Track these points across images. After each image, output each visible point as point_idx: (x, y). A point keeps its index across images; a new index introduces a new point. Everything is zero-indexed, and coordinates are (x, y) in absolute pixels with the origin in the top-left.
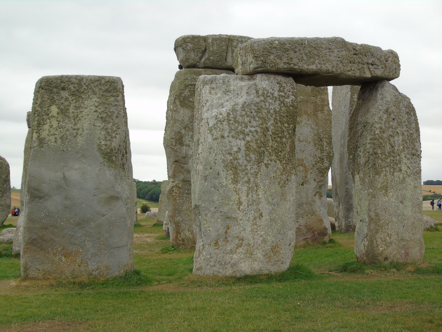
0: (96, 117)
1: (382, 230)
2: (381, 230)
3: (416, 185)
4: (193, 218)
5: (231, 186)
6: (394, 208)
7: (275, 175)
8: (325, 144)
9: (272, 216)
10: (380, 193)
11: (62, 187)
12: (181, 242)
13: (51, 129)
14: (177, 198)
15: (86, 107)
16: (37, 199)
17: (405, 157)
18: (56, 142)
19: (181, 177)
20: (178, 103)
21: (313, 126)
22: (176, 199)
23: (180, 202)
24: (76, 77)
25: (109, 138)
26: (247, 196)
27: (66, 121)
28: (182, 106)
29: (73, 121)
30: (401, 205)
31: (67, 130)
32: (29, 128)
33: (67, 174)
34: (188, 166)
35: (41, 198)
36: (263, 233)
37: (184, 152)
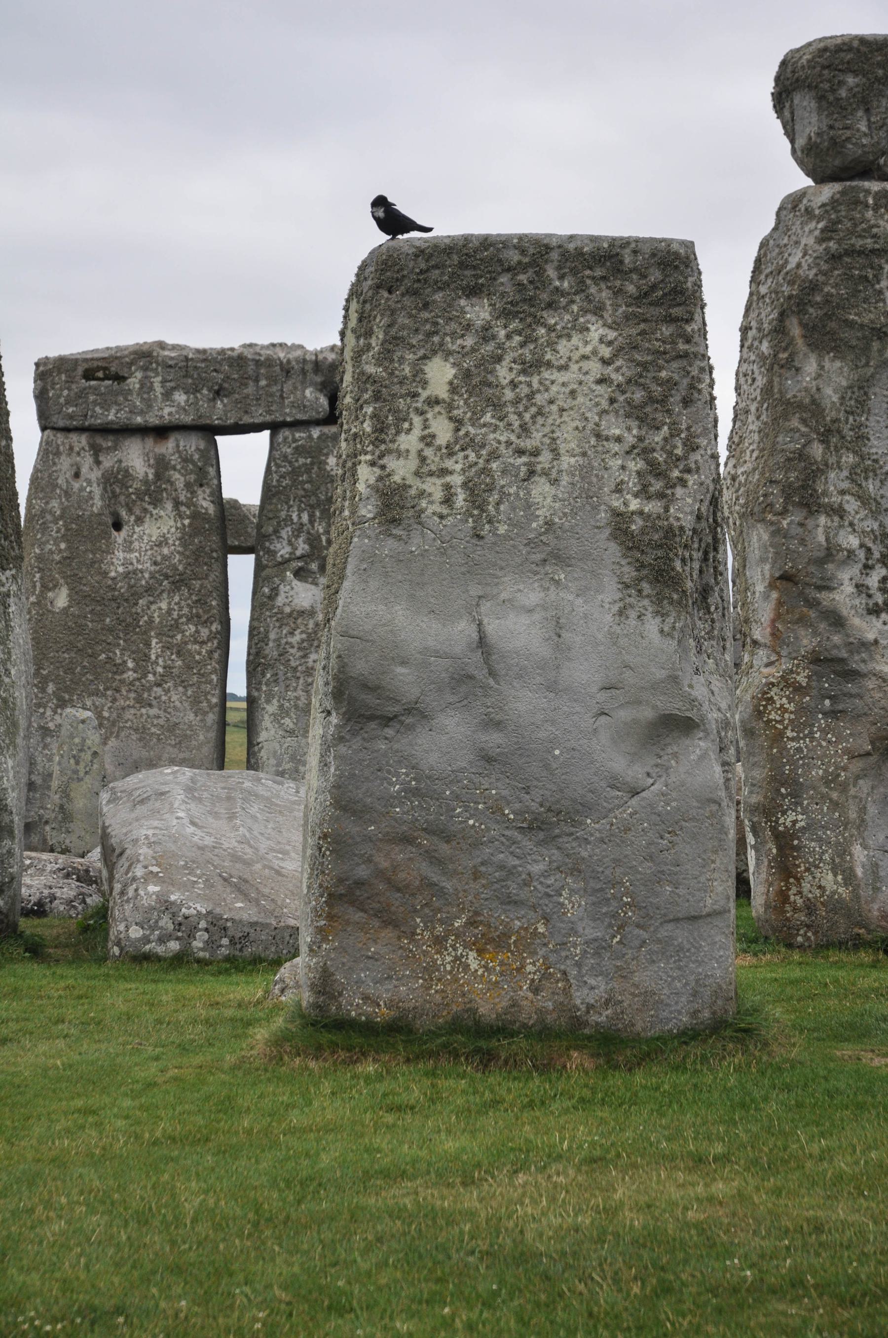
0: (605, 404)
4: (853, 815)
11: (471, 677)
13: (428, 452)
14: (789, 734)
15: (562, 362)
16: (373, 725)
18: (448, 500)
19: (805, 642)
20: (796, 331)
22: (781, 734)
23: (799, 750)
24: (522, 243)
25: (657, 485)
27: (488, 418)
28: (814, 346)
29: (513, 418)
31: (494, 455)
32: (43, 429)
33: (492, 627)
35: (387, 720)
37: (821, 538)
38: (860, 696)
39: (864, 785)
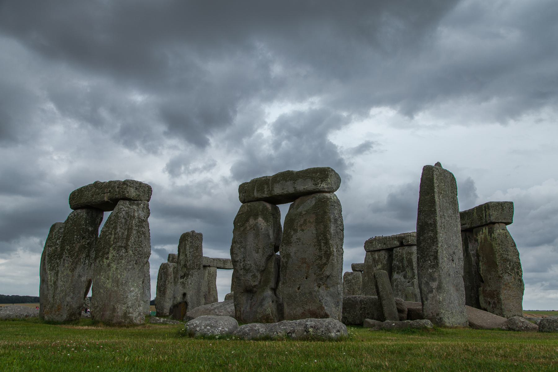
5: (49, 272)
8: (322, 244)
30: (108, 281)
39: (244, 298)
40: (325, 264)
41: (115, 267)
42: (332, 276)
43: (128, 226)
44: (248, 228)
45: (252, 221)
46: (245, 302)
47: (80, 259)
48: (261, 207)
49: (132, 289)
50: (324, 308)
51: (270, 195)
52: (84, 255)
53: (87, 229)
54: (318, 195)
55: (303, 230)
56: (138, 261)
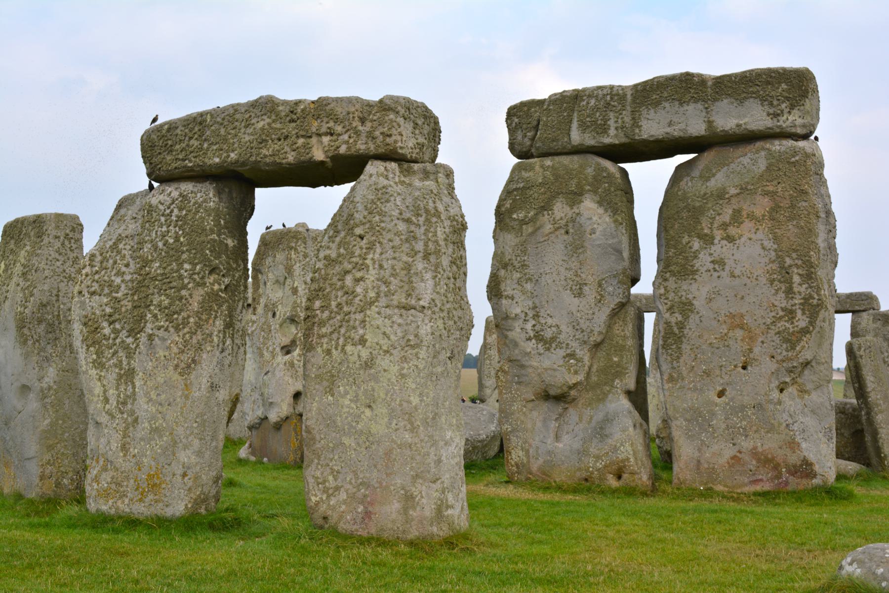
1: (319, 460)
2: (316, 461)
3: (405, 371)
5: (93, 372)
6: (347, 418)
7: (167, 354)
8: (796, 279)
9: (155, 423)
10: (317, 387)
12: (514, 468)
17: (379, 313)
21: (766, 243)
26: (117, 389)
30: (368, 412)
34: (513, 333)
36: (136, 451)
38: (527, 375)
39: (535, 414)
40: (805, 331)
41: (395, 369)
42: (818, 363)
43: (426, 245)
44: (548, 228)
45: (560, 209)
46: (539, 424)
47: (211, 335)
48: (590, 171)
49: (449, 434)
50: (799, 444)
51: (624, 140)
52: (219, 324)
53: (221, 242)
54: (778, 146)
55: (730, 239)
56: (456, 352)
